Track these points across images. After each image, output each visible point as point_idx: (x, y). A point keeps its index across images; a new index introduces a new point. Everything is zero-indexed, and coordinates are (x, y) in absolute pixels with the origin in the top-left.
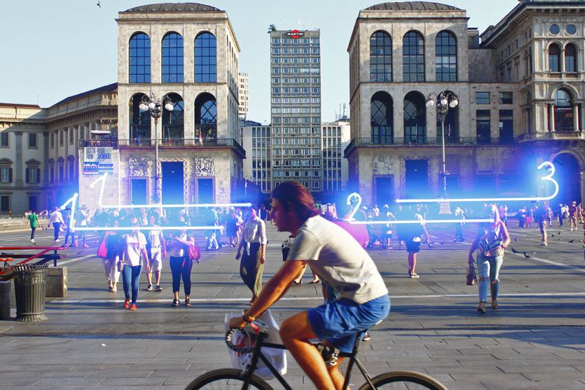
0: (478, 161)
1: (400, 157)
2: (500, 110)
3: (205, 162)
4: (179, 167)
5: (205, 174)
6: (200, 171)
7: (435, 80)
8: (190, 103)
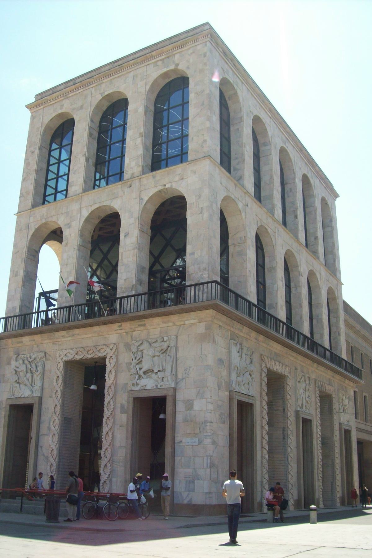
6: (140, 377)
8: (132, 221)
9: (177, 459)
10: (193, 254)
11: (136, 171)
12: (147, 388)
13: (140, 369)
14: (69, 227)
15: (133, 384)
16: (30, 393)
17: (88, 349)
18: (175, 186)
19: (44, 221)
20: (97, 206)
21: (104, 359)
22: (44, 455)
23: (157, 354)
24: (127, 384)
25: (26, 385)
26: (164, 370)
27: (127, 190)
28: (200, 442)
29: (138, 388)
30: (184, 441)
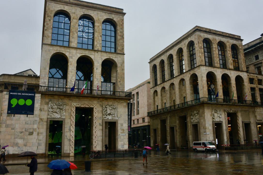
0: (257, 114)
1: (224, 111)
2: (259, 88)
3: (110, 109)
4: (89, 111)
5: (110, 118)
6: (106, 115)
7: (233, 69)
8: (99, 65)
9: (119, 139)
10: (120, 82)
11: (99, 48)
12: (109, 119)
13: (106, 113)
14: (72, 58)
15: (104, 117)
16: (60, 117)
17: (86, 104)
18: (114, 59)
19: (58, 51)
20: (84, 54)
21: (93, 108)
22: (67, 139)
23: (112, 109)
24: (101, 117)
25: (57, 113)
26: (115, 114)
27: (96, 54)
28: (125, 135)
29: (106, 119)
30: (120, 134)
